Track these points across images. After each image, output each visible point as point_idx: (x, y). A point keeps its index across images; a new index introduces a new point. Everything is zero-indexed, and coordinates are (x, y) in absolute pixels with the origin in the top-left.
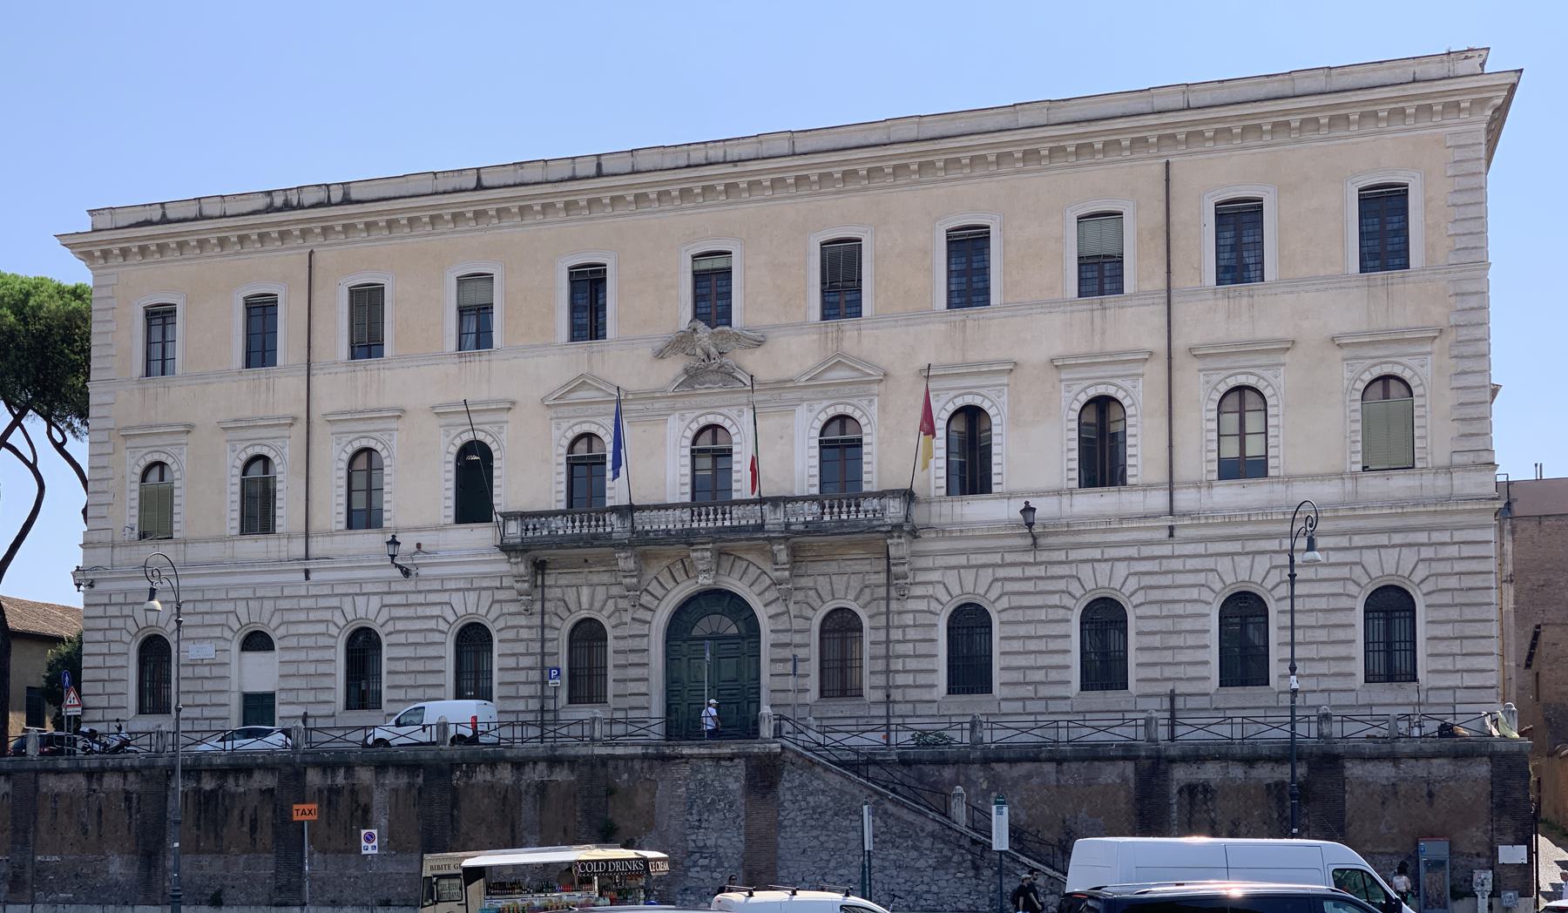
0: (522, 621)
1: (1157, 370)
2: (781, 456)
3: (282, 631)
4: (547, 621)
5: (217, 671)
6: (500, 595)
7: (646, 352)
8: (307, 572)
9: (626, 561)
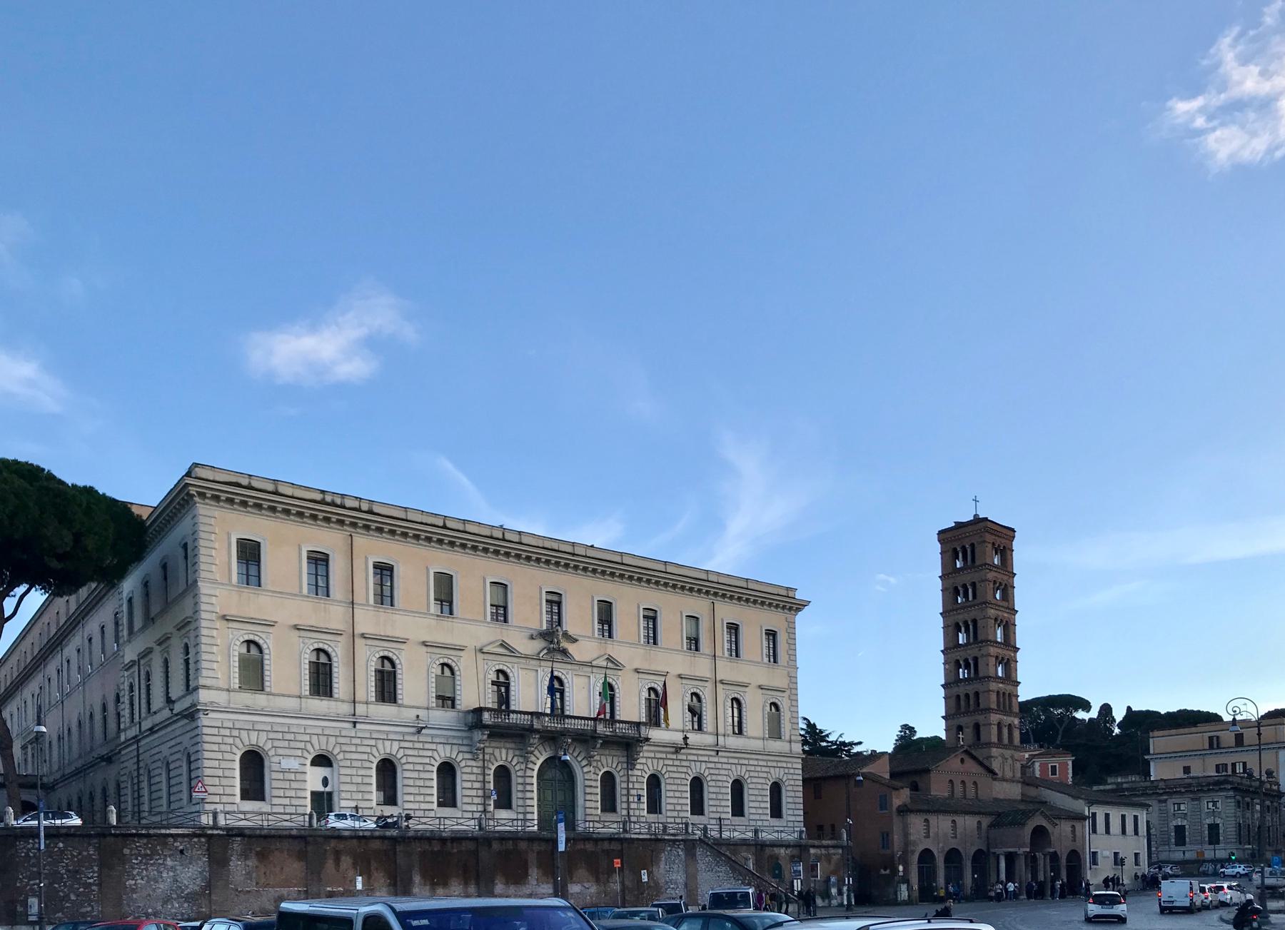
0: (473, 763)
1: (709, 685)
5: (299, 777)
8: (355, 723)
9: (535, 739)
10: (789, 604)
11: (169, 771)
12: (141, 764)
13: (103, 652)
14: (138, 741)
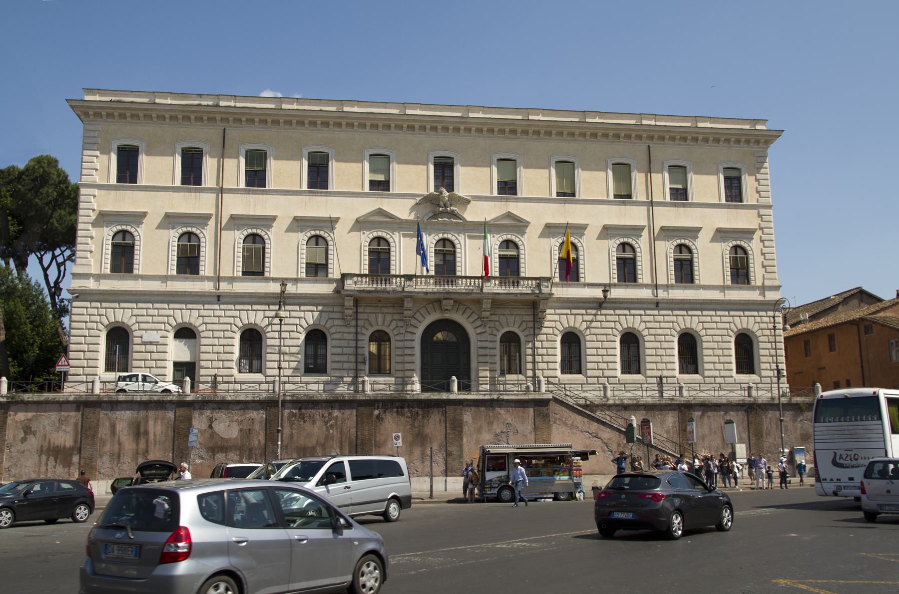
0: (346, 330)
4: (359, 330)
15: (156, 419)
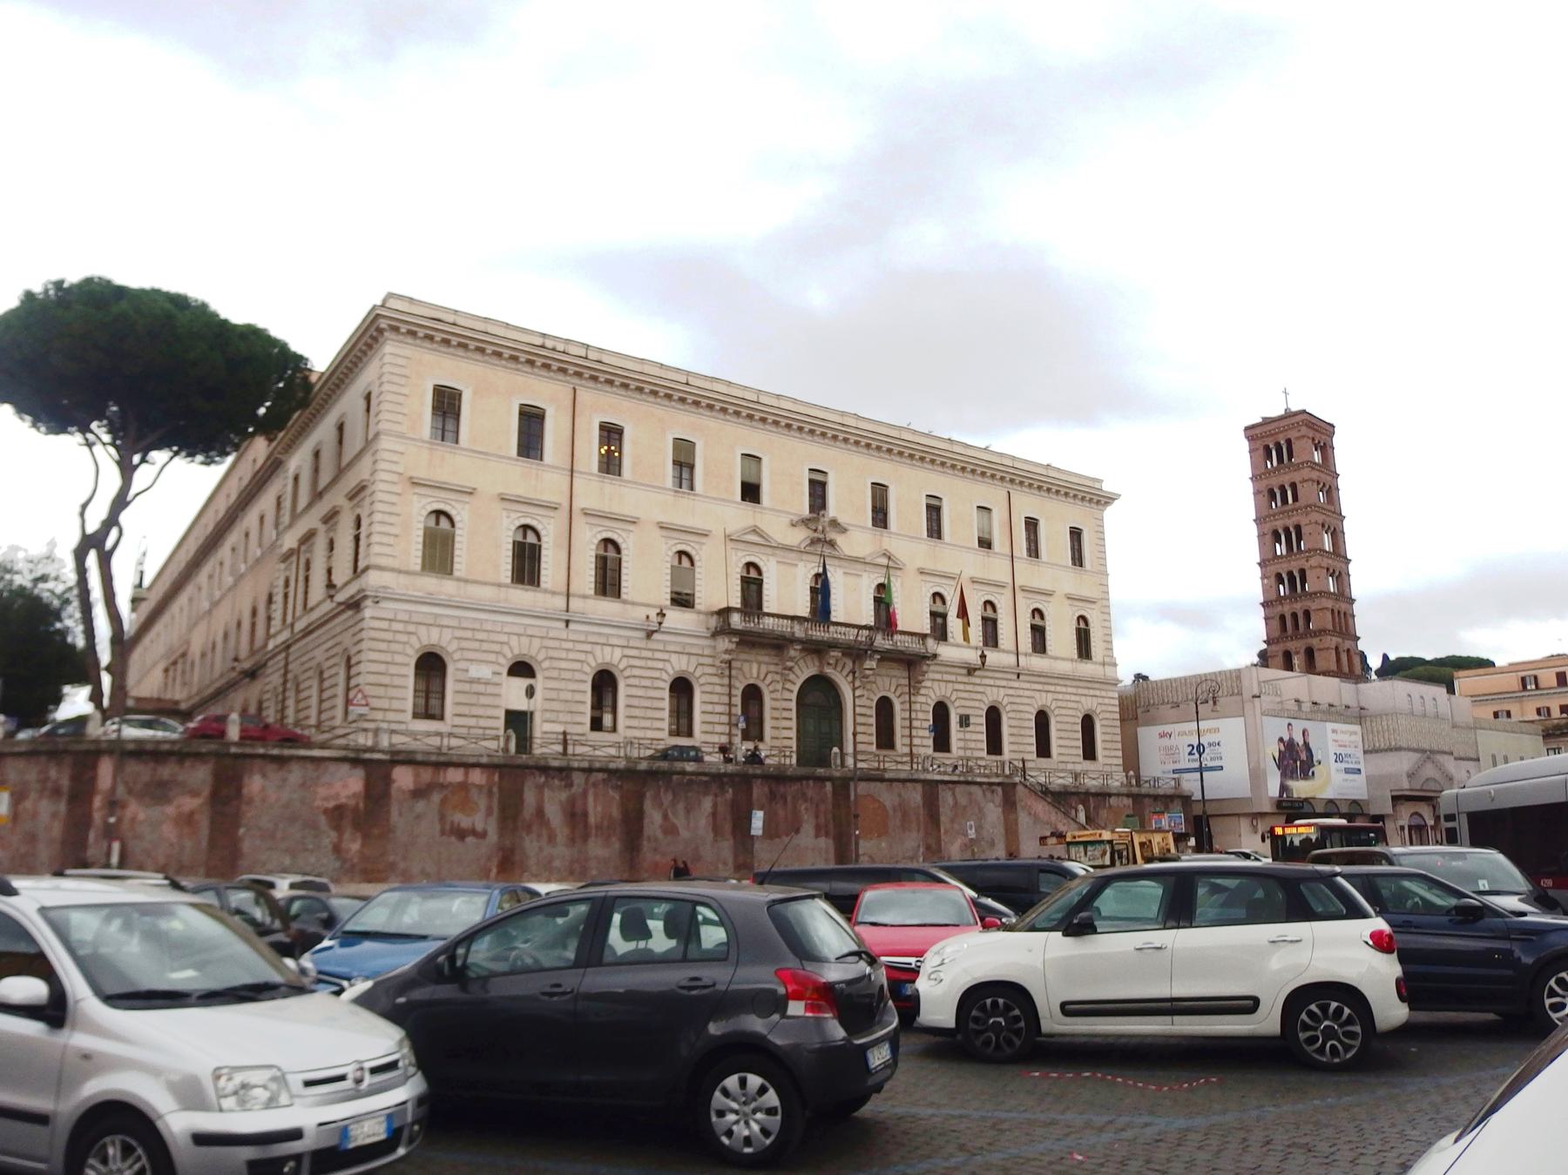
0: (716, 680)
1: (1008, 592)
2: (852, 604)
3: (546, 664)
5: (490, 689)
6: (702, 660)
7: (785, 520)
8: (567, 622)
10: (1095, 498)
11: (322, 681)
12: (290, 676)
13: (260, 545)
14: (288, 647)
15: (596, 796)
